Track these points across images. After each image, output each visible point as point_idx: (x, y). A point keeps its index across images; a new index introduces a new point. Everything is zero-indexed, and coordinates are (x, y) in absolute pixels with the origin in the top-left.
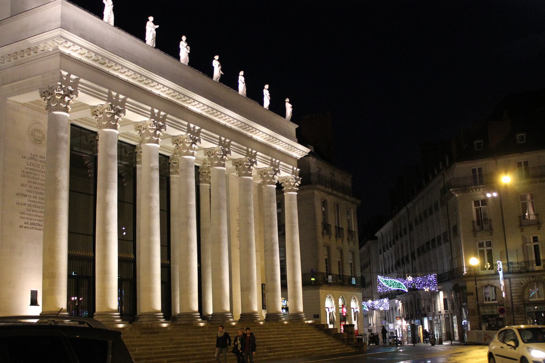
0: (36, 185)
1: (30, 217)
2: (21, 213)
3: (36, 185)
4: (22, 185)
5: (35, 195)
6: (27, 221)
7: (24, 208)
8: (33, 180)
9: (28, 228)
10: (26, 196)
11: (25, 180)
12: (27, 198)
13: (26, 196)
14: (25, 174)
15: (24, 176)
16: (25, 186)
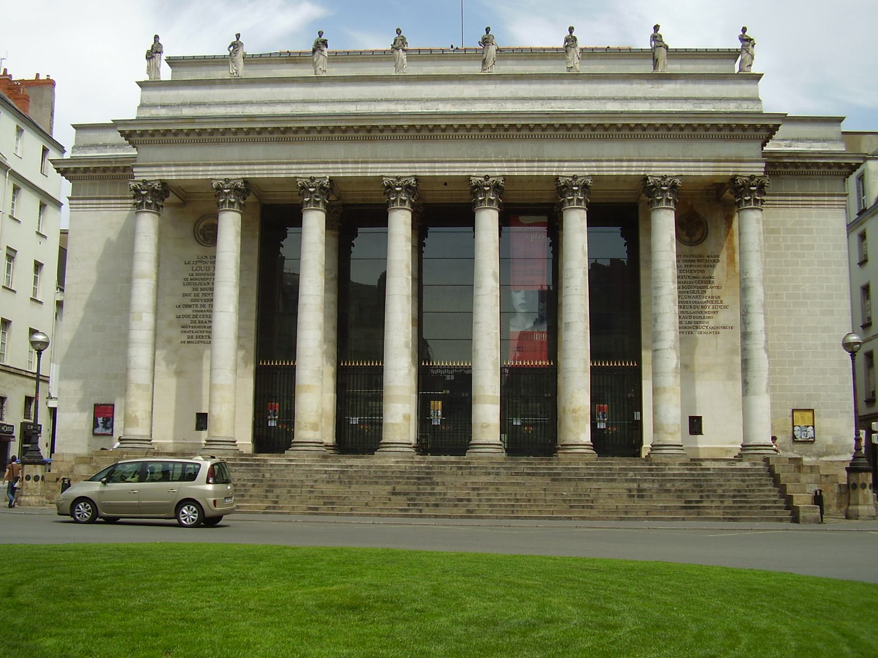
0: (206, 292)
1: (195, 330)
2: (183, 327)
3: (206, 292)
4: (185, 295)
5: (203, 303)
6: (190, 334)
7: (187, 321)
8: (199, 287)
9: (192, 342)
10: (190, 306)
11: (188, 289)
12: (192, 309)
13: (190, 306)
14: (189, 281)
15: (189, 284)
16: (189, 295)
